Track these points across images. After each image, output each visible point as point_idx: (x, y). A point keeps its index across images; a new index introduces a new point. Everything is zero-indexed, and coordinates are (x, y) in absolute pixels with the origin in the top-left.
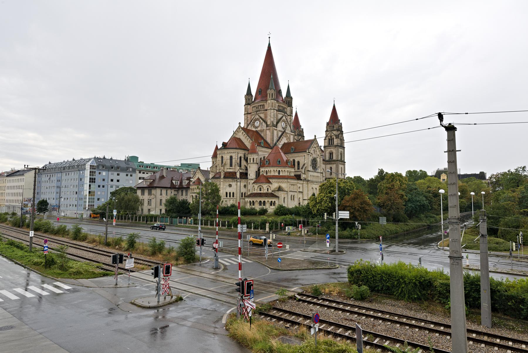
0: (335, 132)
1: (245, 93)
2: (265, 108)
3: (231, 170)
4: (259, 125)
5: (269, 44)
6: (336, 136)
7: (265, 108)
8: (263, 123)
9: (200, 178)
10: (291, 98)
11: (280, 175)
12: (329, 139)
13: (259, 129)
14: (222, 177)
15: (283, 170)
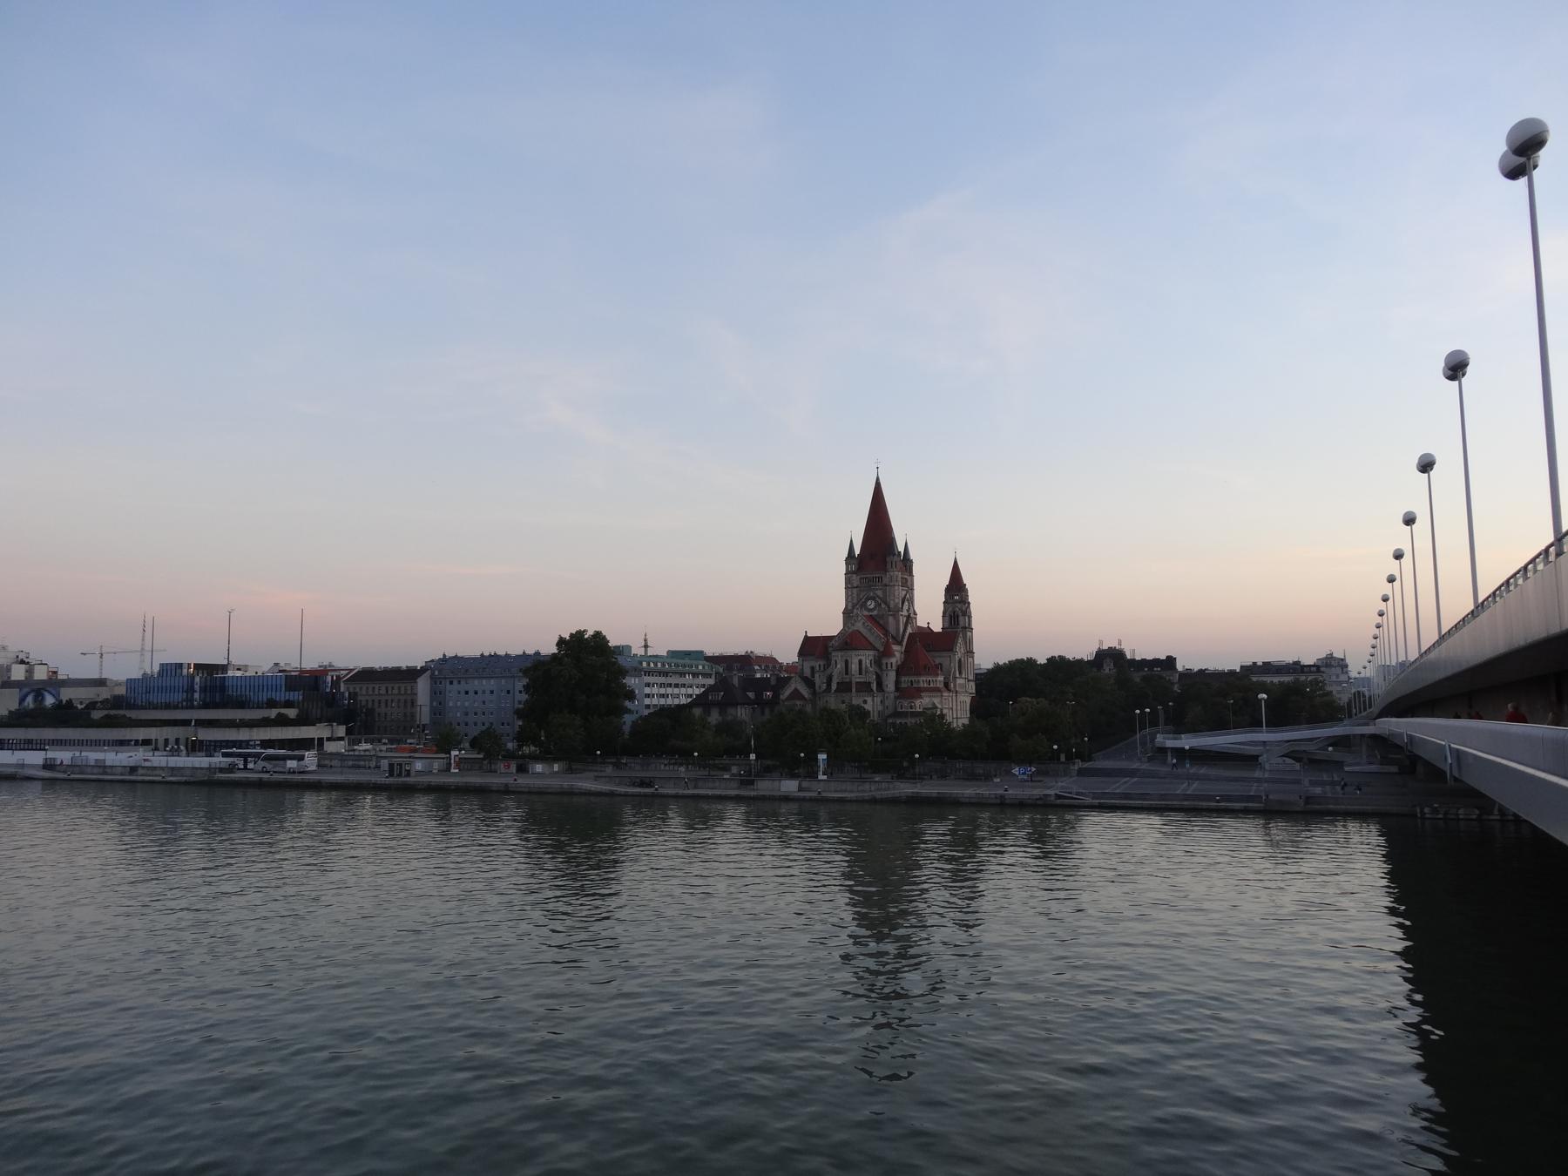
0: (959, 605)
1: (846, 554)
2: (884, 582)
3: (862, 680)
4: (875, 607)
5: (878, 479)
6: (962, 611)
7: (884, 582)
8: (883, 606)
9: (799, 688)
10: (911, 561)
11: (931, 686)
12: (951, 617)
13: (875, 613)
14: (854, 690)
15: (934, 679)
